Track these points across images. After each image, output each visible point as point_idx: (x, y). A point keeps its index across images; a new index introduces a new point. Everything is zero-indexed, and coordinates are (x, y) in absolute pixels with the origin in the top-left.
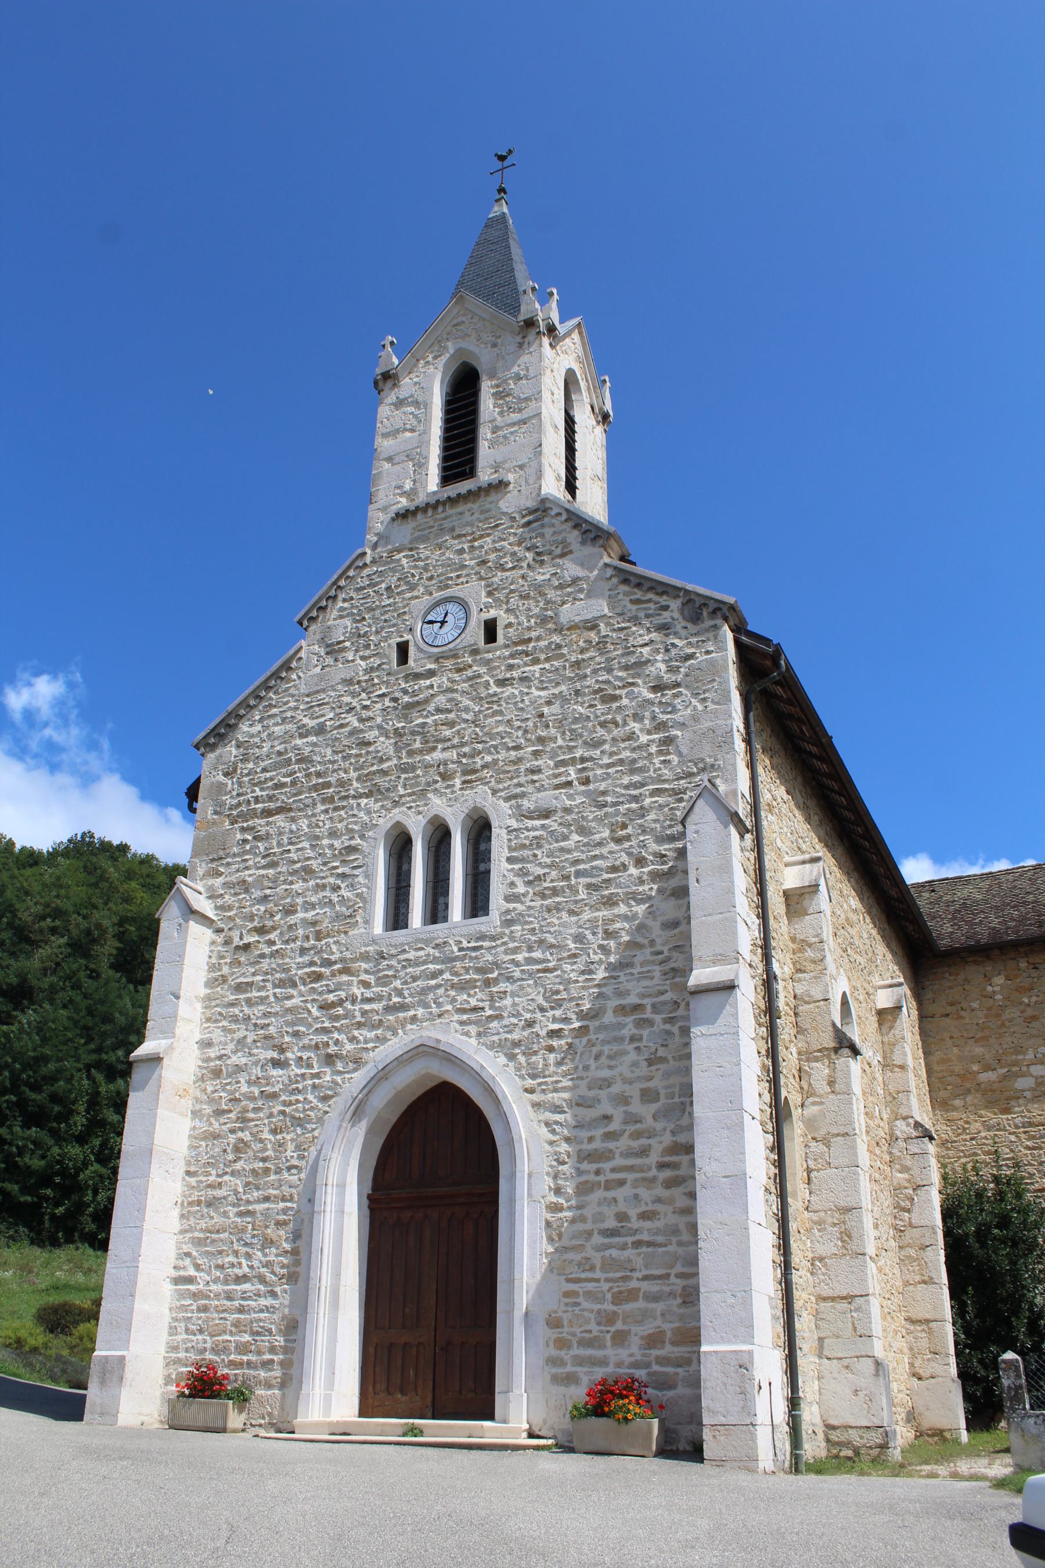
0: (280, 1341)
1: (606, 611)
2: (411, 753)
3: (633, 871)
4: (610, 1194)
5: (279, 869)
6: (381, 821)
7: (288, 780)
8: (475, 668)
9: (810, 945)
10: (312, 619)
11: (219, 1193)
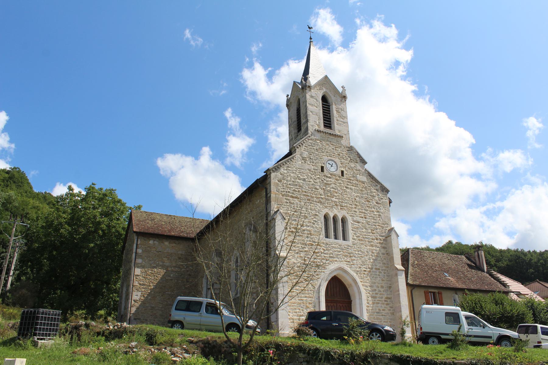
2: (328, 196)
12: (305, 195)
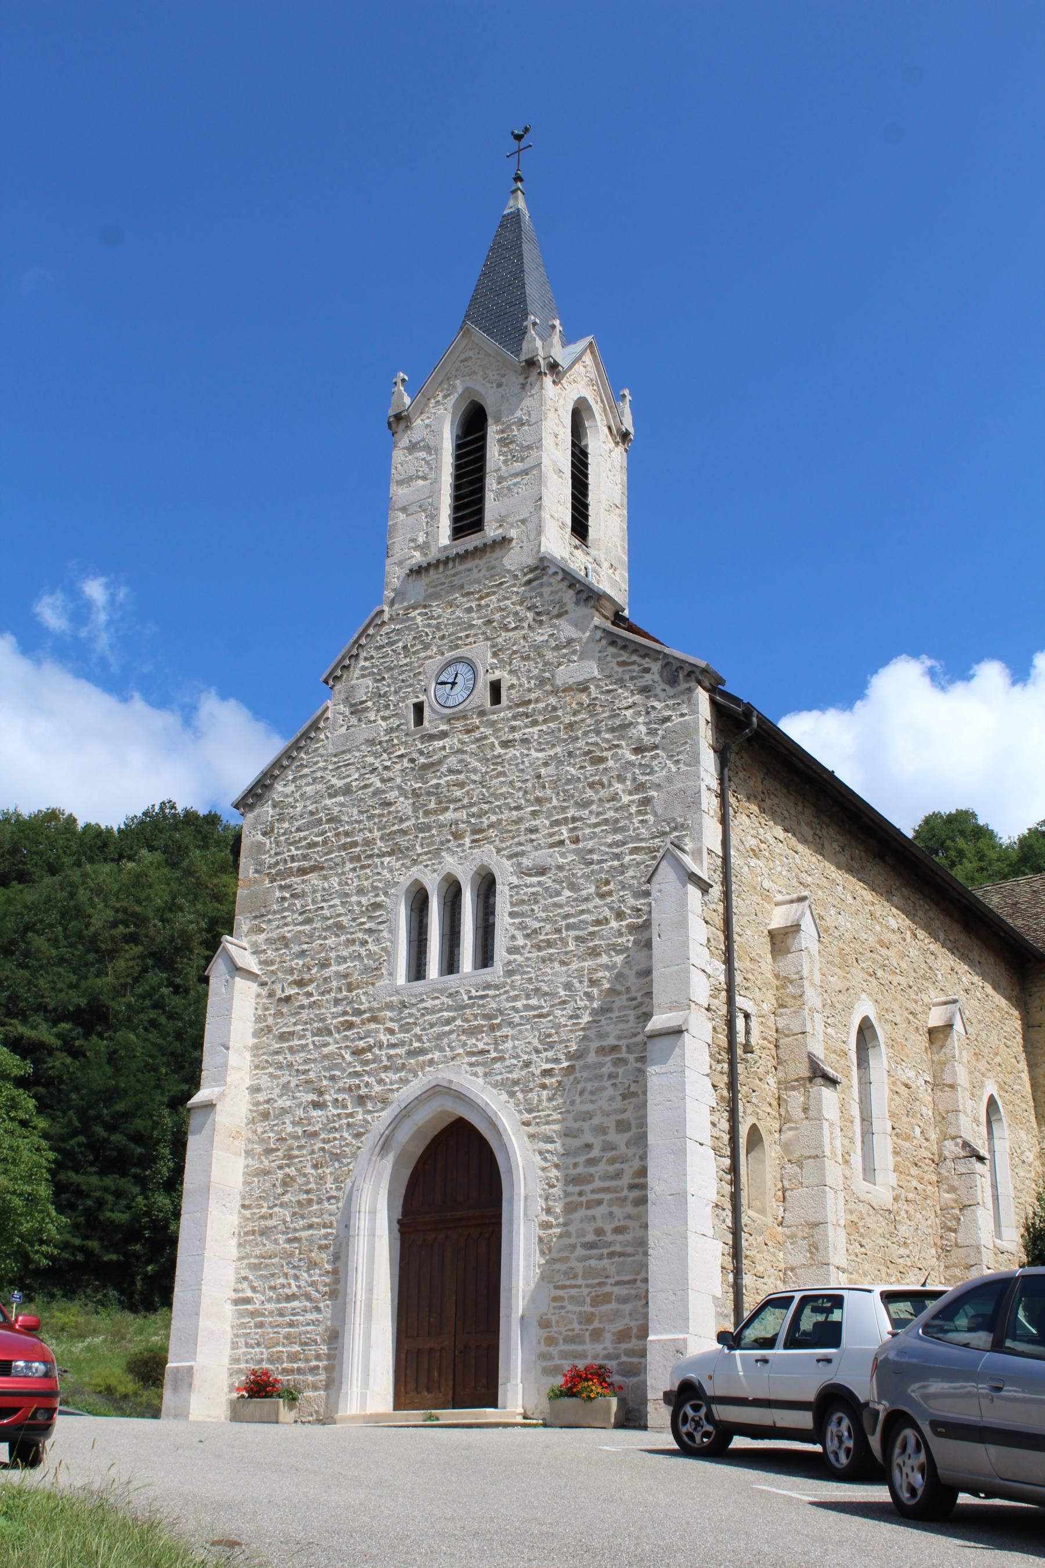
0: (324, 1349)
1: (596, 673)
2: (427, 813)
3: (614, 924)
4: (590, 1212)
5: (314, 925)
6: (402, 878)
7: (320, 839)
8: (482, 730)
9: (791, 982)
10: (337, 678)
11: (270, 1223)
12: (344, 847)
